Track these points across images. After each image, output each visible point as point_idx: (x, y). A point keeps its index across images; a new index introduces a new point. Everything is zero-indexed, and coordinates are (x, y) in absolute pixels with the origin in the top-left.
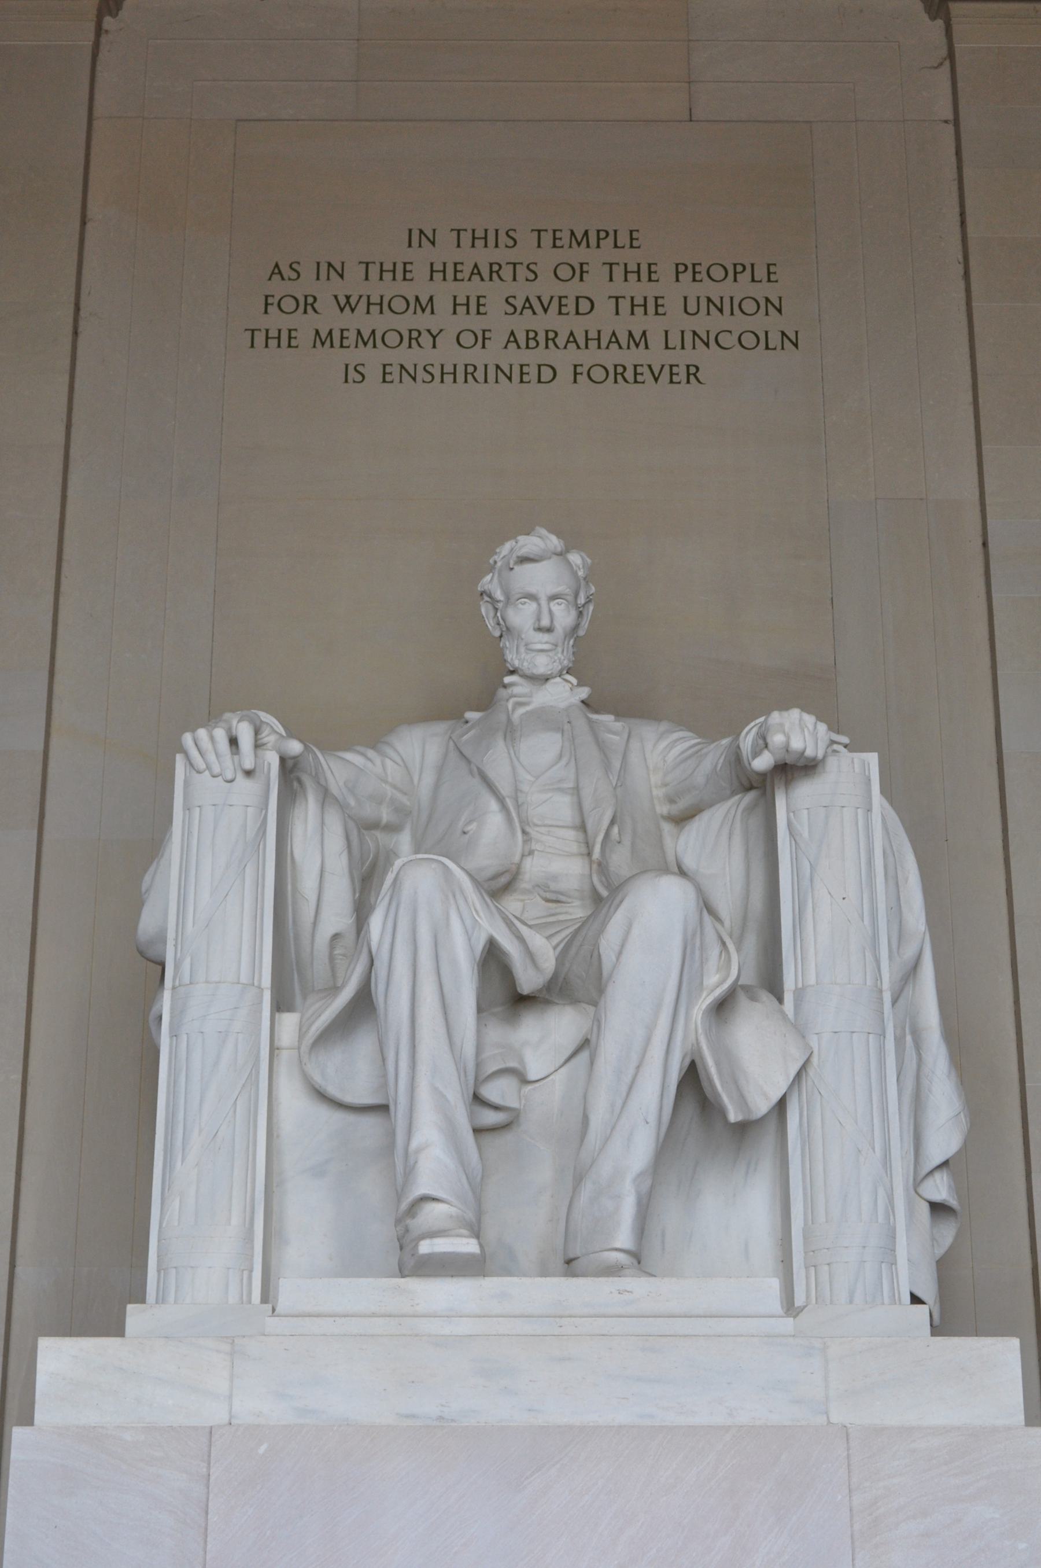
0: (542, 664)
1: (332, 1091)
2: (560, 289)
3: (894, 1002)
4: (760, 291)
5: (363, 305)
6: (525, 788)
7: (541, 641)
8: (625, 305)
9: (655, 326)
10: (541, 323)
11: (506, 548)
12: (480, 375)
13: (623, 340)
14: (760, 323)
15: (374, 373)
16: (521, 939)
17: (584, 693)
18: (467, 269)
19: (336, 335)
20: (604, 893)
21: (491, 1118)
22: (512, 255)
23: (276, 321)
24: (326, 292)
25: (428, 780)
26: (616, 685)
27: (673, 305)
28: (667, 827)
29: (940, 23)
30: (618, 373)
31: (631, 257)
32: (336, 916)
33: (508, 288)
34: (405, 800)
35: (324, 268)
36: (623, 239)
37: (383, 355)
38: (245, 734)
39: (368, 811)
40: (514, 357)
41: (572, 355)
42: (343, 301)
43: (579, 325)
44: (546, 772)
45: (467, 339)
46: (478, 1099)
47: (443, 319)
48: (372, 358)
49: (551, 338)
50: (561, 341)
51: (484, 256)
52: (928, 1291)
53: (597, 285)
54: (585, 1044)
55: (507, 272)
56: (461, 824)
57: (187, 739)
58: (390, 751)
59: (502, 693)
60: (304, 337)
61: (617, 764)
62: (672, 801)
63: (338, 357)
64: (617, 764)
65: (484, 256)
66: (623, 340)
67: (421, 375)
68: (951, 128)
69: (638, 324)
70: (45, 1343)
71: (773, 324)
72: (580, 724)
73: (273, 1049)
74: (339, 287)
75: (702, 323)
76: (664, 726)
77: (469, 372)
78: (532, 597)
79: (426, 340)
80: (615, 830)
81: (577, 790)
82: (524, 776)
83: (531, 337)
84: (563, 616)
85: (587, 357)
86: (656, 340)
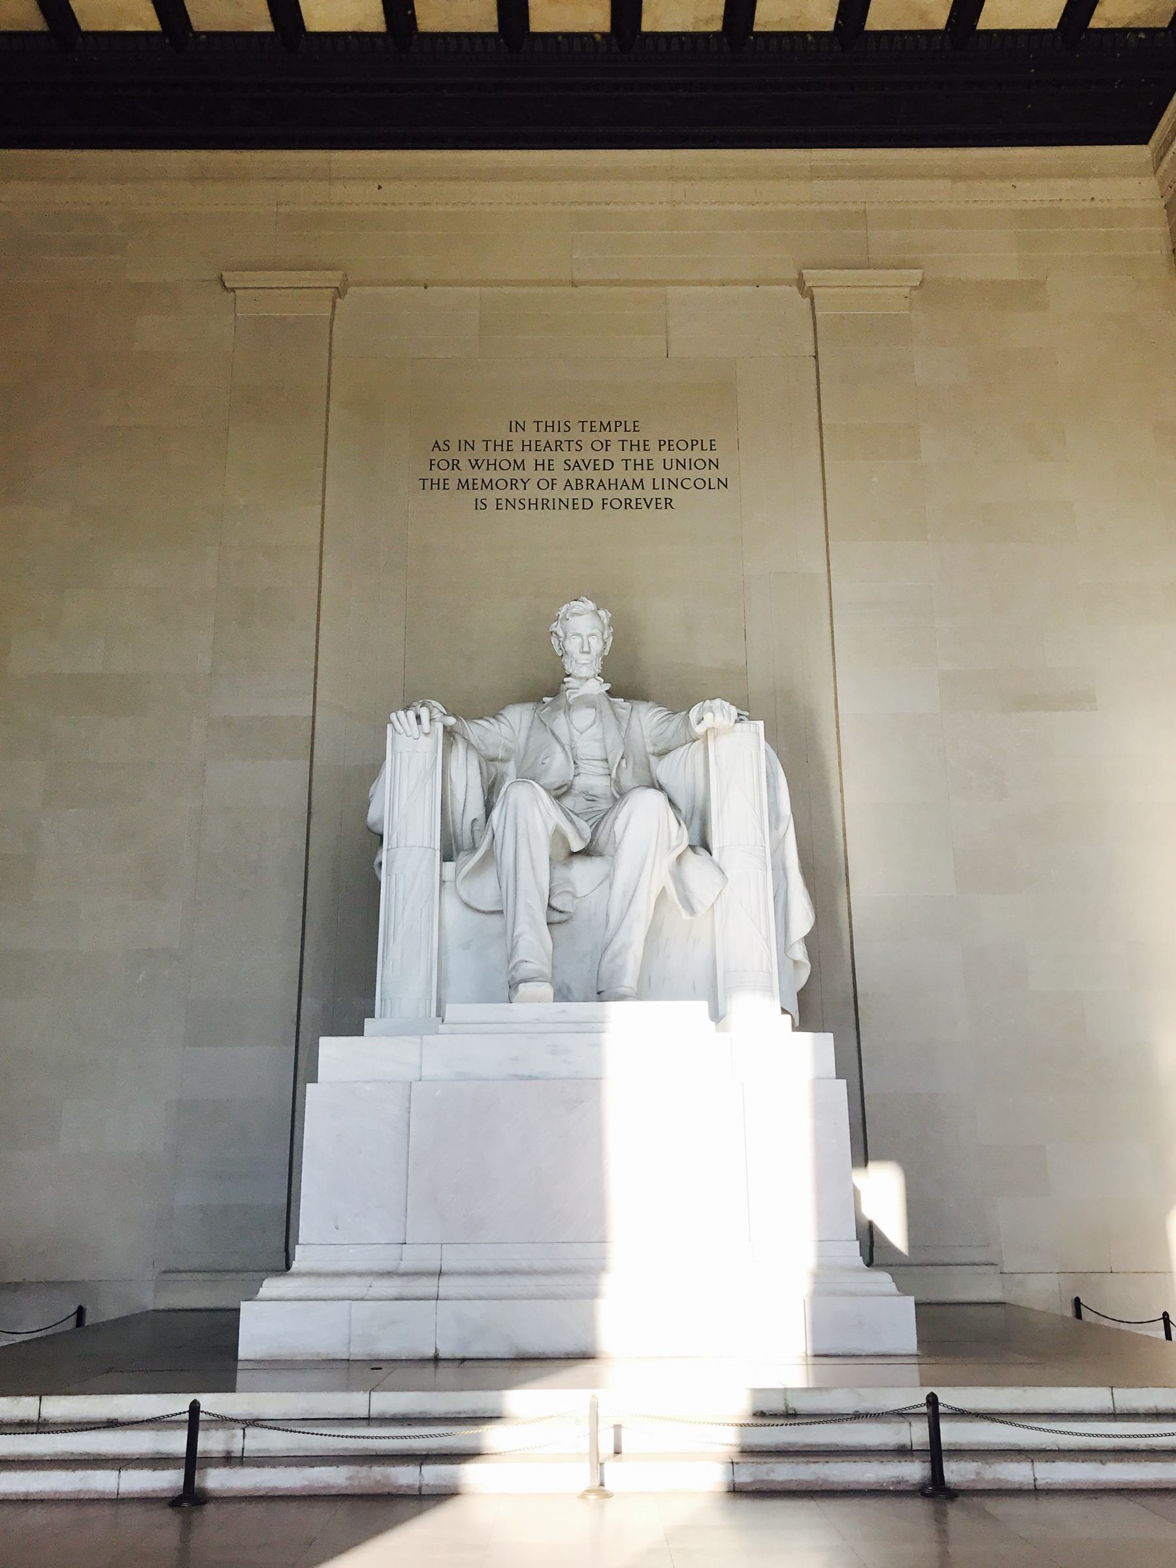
0: (585, 672)
1: (473, 904)
2: (594, 455)
3: (772, 855)
4: (706, 455)
5: (484, 466)
6: (576, 739)
7: (584, 658)
8: (631, 464)
9: (647, 476)
10: (584, 475)
11: (564, 608)
12: (550, 505)
13: (630, 484)
14: (706, 474)
15: (491, 504)
16: (572, 821)
17: (607, 686)
18: (543, 444)
19: (471, 482)
20: (618, 796)
21: (556, 917)
22: (568, 436)
23: (436, 474)
24: (464, 458)
25: (523, 734)
26: (625, 683)
27: (657, 465)
28: (653, 759)
29: (808, 300)
30: (627, 503)
31: (635, 437)
32: (475, 809)
33: (566, 455)
34: (512, 745)
35: (463, 443)
36: (630, 426)
37: (497, 494)
38: (424, 713)
39: (491, 752)
40: (569, 494)
41: (602, 493)
42: (474, 463)
43: (605, 476)
44: (587, 731)
45: (543, 484)
46: (550, 906)
47: (529, 473)
48: (491, 496)
49: (590, 484)
50: (595, 485)
51: (552, 437)
52: (794, 1007)
53: (615, 453)
54: (608, 876)
55: (565, 446)
56: (540, 761)
57: (393, 716)
58: (503, 720)
59: (564, 687)
60: (453, 484)
61: (625, 726)
62: (655, 745)
63: (470, 496)
64: (625, 726)
65: (552, 437)
66: (630, 484)
67: (518, 505)
68: (813, 360)
69: (638, 475)
70: (323, 1041)
71: (712, 474)
72: (606, 704)
73: (442, 882)
75: (675, 474)
76: (651, 704)
77: (545, 503)
78: (579, 635)
79: (520, 485)
80: (624, 762)
81: (603, 740)
82: (575, 732)
83: (579, 482)
84: (596, 645)
85: (610, 494)
86: (648, 484)
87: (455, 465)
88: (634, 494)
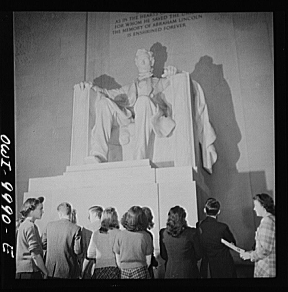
15: (132, 34)
23: (117, 29)
30: (172, 27)
40: (155, 27)
41: (164, 25)
47: (143, 24)
48: (132, 32)
60: (122, 31)
63: (126, 33)
67: (140, 33)
72: (149, 80)
74: (127, 22)
77: (147, 32)
83: (157, 24)
85: (166, 26)
86: (178, 21)
87: (122, 26)
88: (173, 24)
